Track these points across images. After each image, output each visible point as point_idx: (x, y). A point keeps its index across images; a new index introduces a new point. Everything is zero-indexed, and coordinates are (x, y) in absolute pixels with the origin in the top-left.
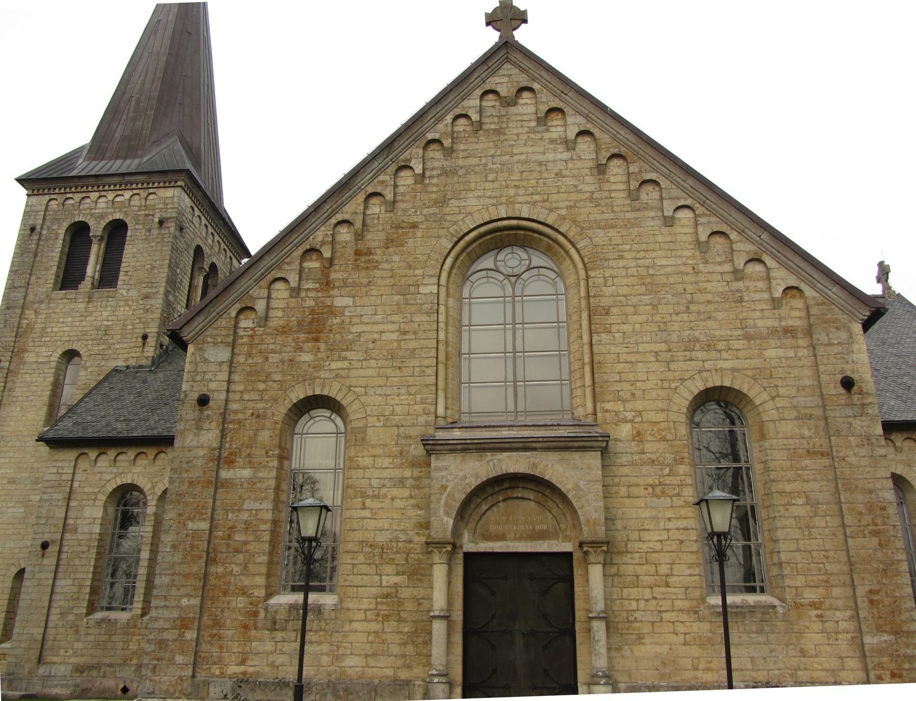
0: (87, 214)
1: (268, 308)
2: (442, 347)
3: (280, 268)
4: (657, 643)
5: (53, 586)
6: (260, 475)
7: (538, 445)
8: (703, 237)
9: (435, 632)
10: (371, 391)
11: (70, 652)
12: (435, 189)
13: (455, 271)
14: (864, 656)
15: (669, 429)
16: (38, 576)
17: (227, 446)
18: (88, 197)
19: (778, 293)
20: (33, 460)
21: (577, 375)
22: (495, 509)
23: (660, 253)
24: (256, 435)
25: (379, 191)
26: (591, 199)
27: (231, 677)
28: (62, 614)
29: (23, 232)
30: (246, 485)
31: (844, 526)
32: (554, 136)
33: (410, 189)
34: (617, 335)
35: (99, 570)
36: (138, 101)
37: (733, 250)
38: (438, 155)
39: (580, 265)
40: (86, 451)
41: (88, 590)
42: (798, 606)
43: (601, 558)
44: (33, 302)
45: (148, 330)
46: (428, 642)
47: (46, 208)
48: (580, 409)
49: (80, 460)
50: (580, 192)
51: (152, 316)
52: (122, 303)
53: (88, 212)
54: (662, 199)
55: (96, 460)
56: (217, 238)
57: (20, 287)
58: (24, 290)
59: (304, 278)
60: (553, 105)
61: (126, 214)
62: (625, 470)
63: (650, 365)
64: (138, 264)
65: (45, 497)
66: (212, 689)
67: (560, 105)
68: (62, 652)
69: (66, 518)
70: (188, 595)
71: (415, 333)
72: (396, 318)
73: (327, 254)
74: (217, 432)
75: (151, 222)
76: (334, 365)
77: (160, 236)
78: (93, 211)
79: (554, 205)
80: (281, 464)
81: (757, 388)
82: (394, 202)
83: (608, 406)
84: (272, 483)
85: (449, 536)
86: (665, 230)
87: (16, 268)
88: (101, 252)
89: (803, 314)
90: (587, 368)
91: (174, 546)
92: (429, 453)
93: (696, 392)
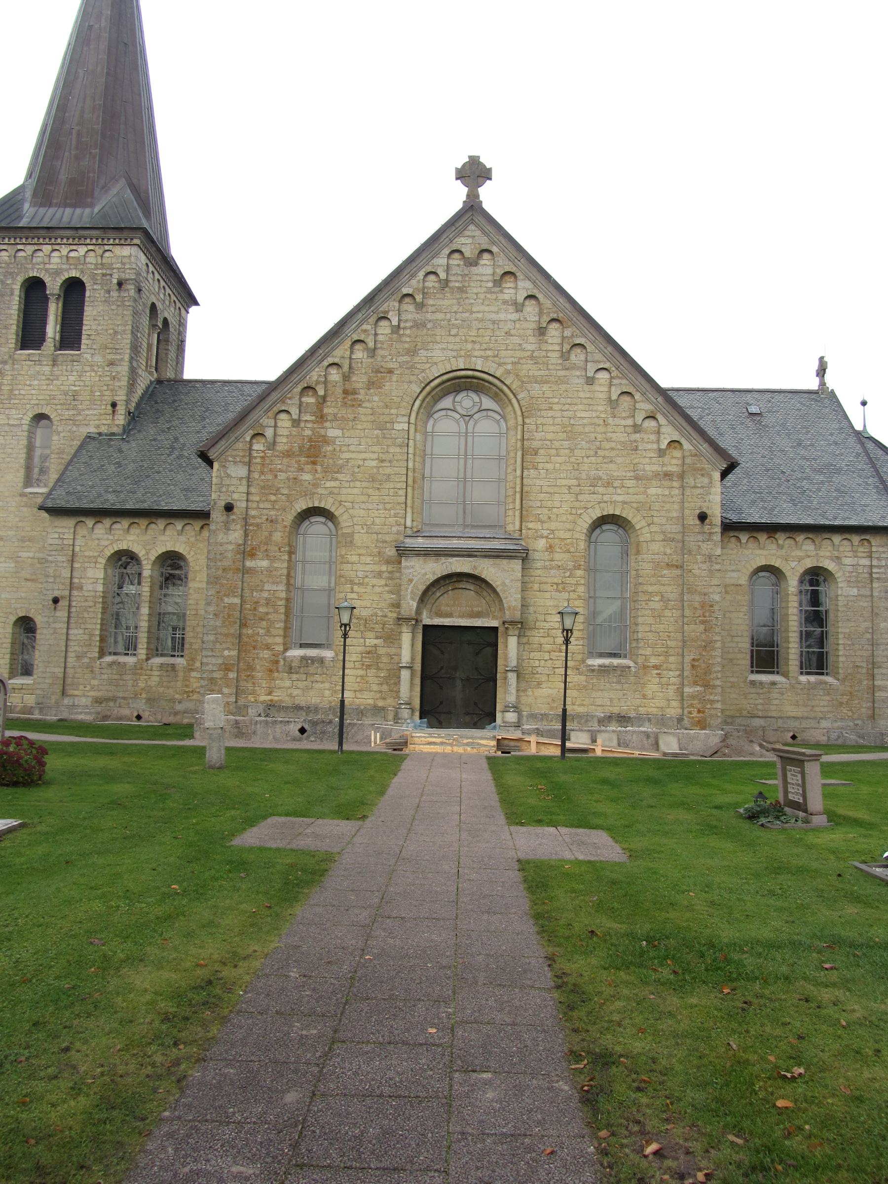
1: (275, 435)
2: (410, 474)
3: (284, 402)
4: (550, 688)
5: (67, 634)
6: (275, 565)
7: (478, 554)
8: (614, 397)
9: (402, 677)
10: (357, 506)
11: (88, 688)
12: (408, 339)
13: (422, 410)
14: (683, 700)
15: (572, 544)
16: (53, 625)
17: (249, 542)
19: (663, 446)
20: (17, 519)
21: (510, 500)
22: (445, 595)
23: (580, 407)
24: (271, 535)
25: (362, 339)
26: (532, 357)
27: (262, 703)
28: (78, 657)
30: (265, 572)
31: (683, 616)
32: (507, 297)
33: (387, 339)
34: (542, 471)
35: (105, 622)
36: (79, 134)
37: (636, 409)
38: (411, 308)
39: (519, 413)
40: (83, 519)
41: (98, 638)
42: (645, 667)
43: (517, 632)
45: (117, 398)
46: (398, 683)
48: (510, 525)
49: (78, 528)
50: (523, 350)
53: (41, 267)
54: (586, 361)
55: (93, 528)
56: (168, 291)
59: (303, 411)
60: (507, 269)
62: (538, 572)
63: (563, 496)
64: (100, 328)
65: (50, 558)
66: (250, 710)
67: (514, 270)
68: (81, 687)
69: (71, 578)
70: (228, 649)
71: (390, 461)
72: (375, 449)
73: (321, 392)
74: (242, 532)
76: (328, 484)
78: (47, 266)
79: (502, 361)
80: (290, 557)
81: (639, 517)
82: (375, 349)
83: (531, 525)
84: (285, 572)
85: (413, 614)
86: (586, 388)
89: (680, 462)
90: (518, 496)
91: (215, 615)
92: (400, 555)
93: (595, 518)
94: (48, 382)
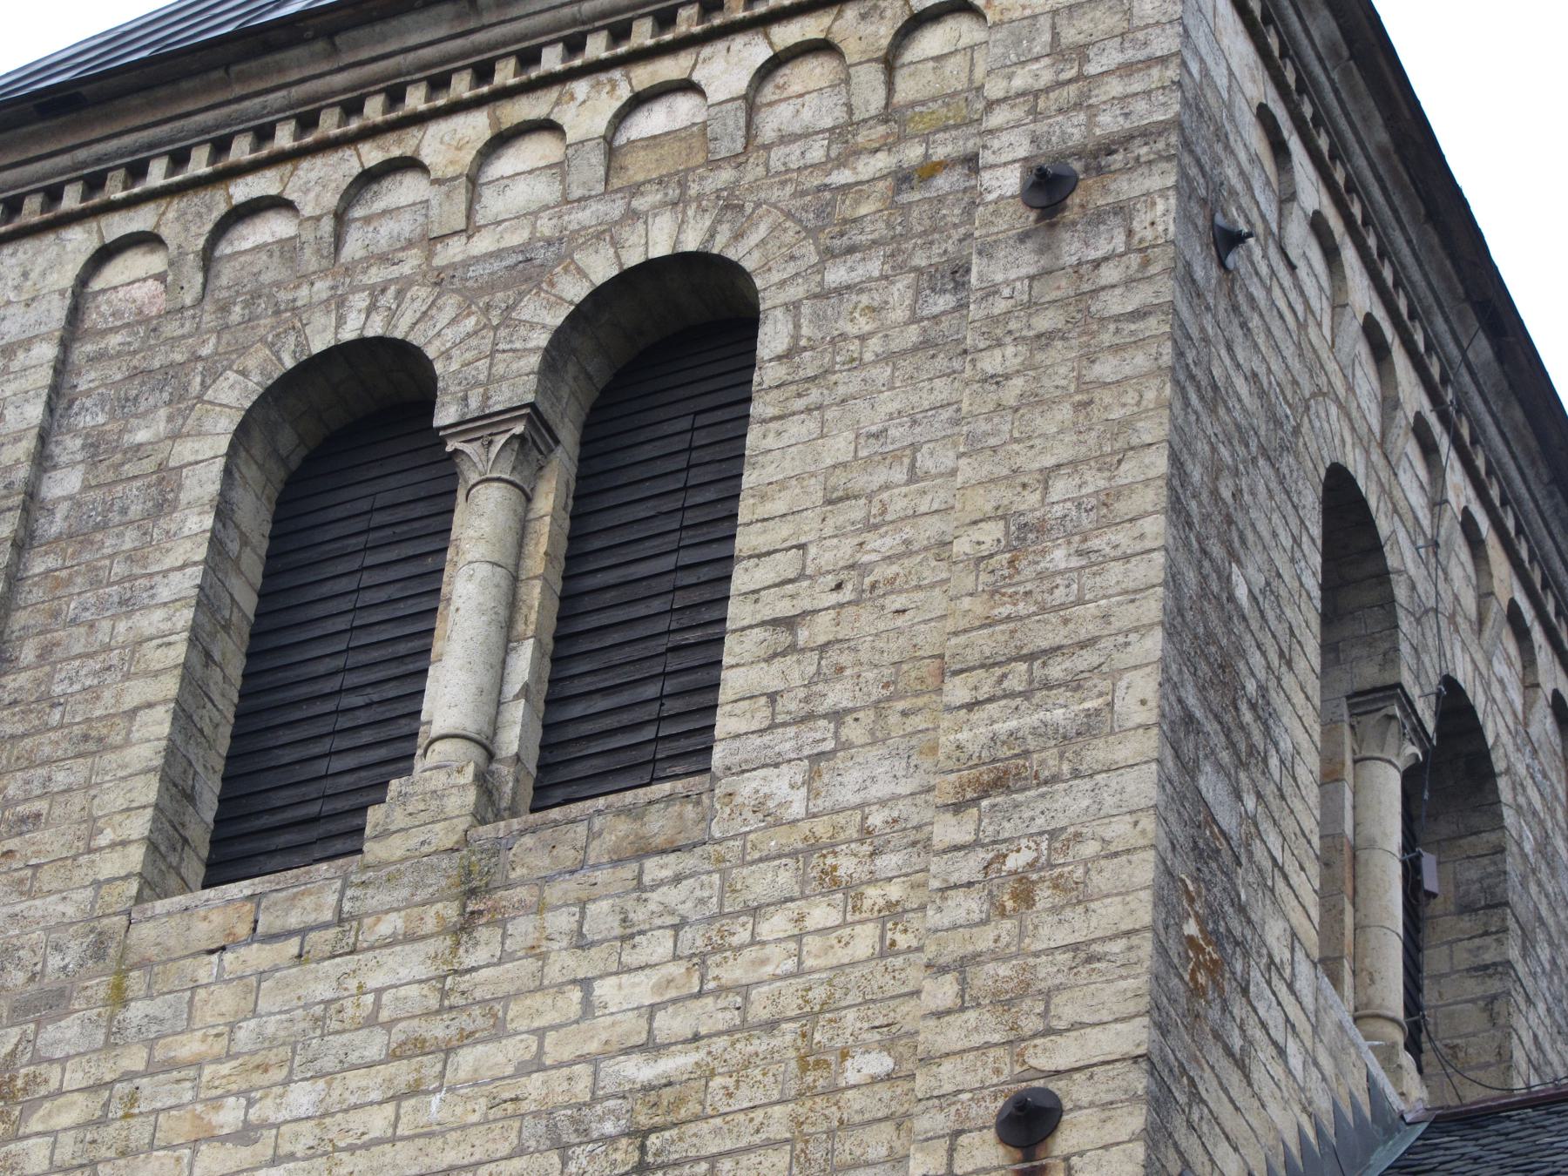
0: (404, 286)
18: (410, 164)
47: (75, 313)
51: (1076, 927)
52: (762, 882)
61: (730, 205)
64: (883, 543)
75: (953, 214)
77: (1063, 286)
78: (454, 251)
88: (535, 562)
94: (402, 1072)
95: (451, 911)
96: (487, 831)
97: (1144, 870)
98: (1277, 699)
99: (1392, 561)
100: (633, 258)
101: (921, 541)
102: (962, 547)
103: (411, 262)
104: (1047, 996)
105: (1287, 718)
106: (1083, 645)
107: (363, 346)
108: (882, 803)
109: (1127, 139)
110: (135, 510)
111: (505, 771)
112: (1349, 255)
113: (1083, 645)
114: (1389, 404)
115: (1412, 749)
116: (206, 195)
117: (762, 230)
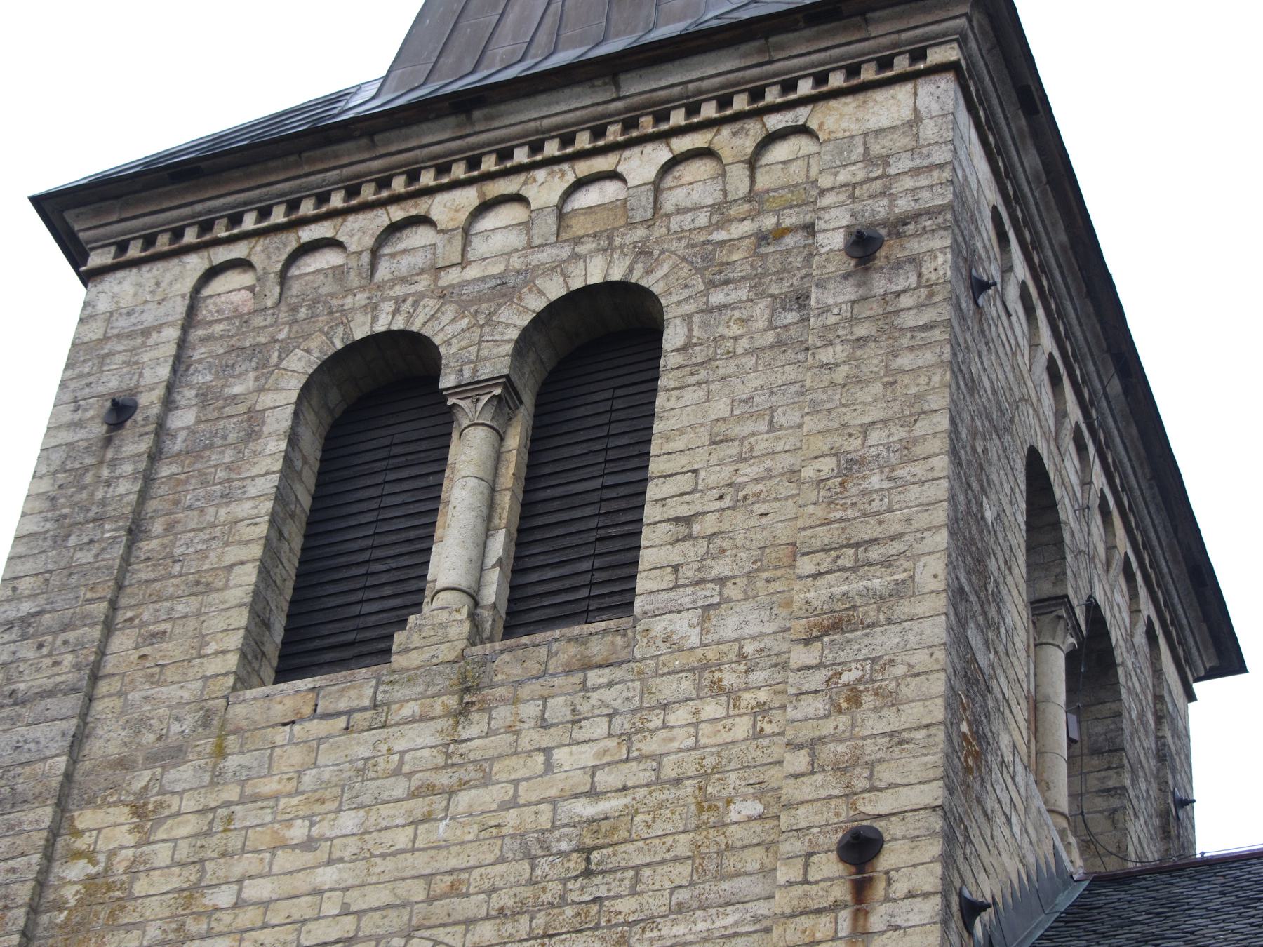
0: (418, 298)
29: (65, 436)
44: (124, 764)
47: (192, 310)
51: (892, 721)
52: (670, 688)
57: (50, 693)
58: (72, 703)
61: (642, 251)
75: (797, 261)
77: (875, 308)
78: (453, 276)
87: (26, 607)
94: (419, 806)
95: (453, 702)
96: (477, 650)
97: (938, 684)
98: (1004, 592)
99: (1062, 516)
100: (576, 284)
101: (778, 469)
102: (808, 473)
103: (423, 283)
104: (872, 766)
105: (1009, 605)
106: (893, 538)
107: (389, 335)
108: (753, 638)
109: (917, 216)
110: (232, 437)
111: (486, 614)
112: (1040, 312)
113: (893, 538)
114: (1061, 414)
115: (1071, 640)
116: (282, 236)
117: (665, 269)
